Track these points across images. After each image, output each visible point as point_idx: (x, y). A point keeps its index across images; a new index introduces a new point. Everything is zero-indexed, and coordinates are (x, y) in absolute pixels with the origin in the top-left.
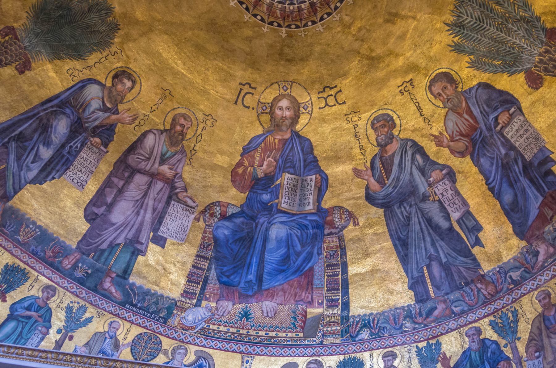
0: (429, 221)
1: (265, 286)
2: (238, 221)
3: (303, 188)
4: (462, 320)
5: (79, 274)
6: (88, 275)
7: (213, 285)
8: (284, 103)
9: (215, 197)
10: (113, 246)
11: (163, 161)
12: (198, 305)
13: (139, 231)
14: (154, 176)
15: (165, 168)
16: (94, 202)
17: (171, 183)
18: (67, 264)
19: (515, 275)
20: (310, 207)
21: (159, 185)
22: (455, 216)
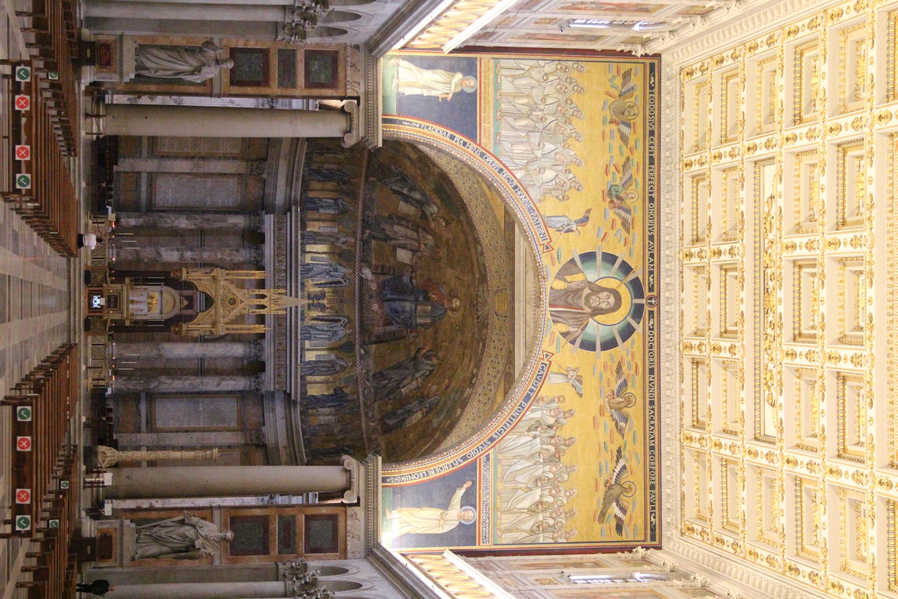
0: (404, 379)
1: (385, 304)
2: (411, 286)
3: (426, 317)
4: (361, 393)
5: (366, 219)
6: (367, 222)
7: (383, 278)
8: (458, 303)
9: (419, 272)
10: (383, 229)
11: (425, 245)
12: (373, 273)
13: (396, 239)
14: (418, 241)
15: (423, 246)
16: (397, 217)
17: (418, 250)
18: (367, 213)
19: (370, 414)
20: (419, 321)
21: (416, 244)
22: (403, 390)
